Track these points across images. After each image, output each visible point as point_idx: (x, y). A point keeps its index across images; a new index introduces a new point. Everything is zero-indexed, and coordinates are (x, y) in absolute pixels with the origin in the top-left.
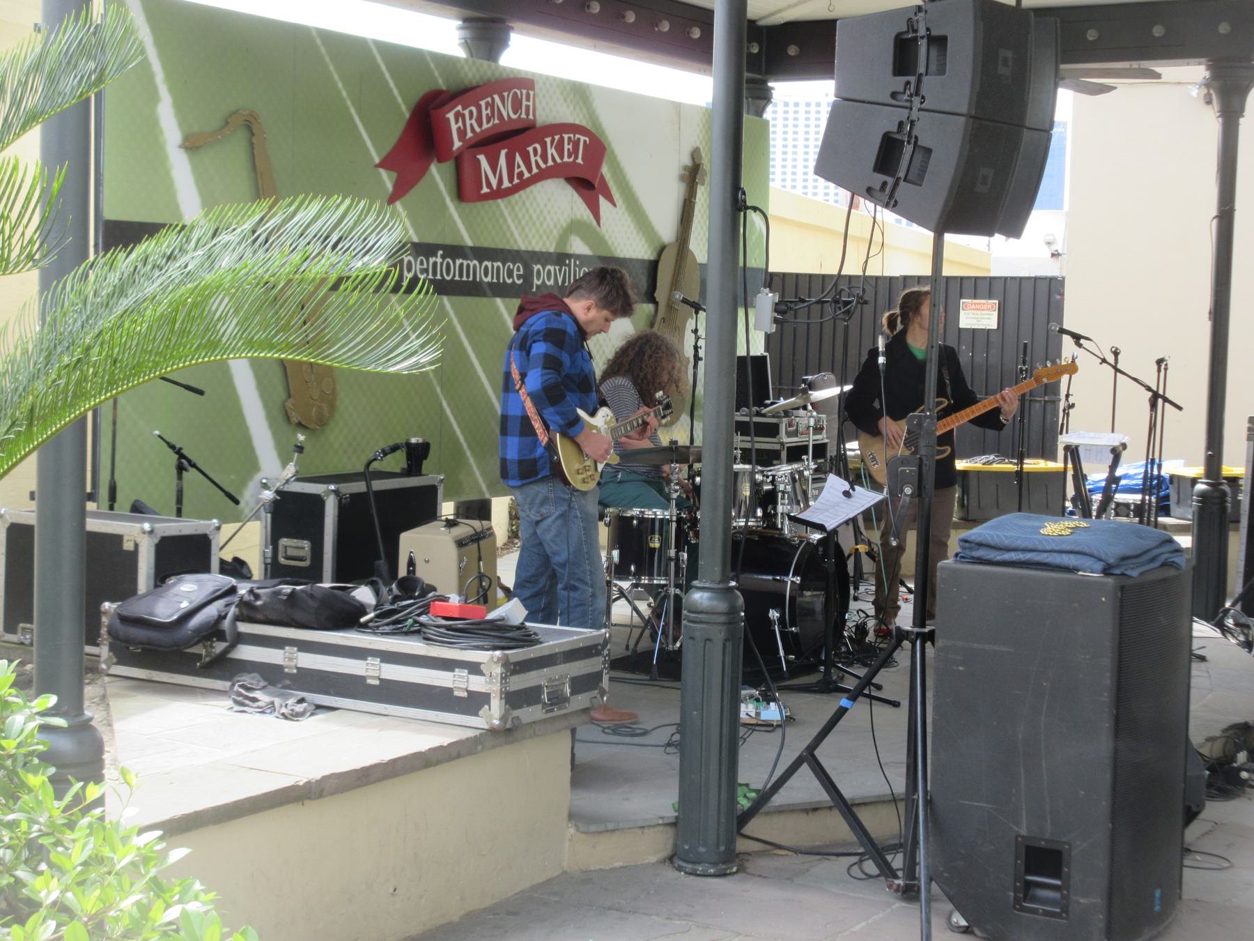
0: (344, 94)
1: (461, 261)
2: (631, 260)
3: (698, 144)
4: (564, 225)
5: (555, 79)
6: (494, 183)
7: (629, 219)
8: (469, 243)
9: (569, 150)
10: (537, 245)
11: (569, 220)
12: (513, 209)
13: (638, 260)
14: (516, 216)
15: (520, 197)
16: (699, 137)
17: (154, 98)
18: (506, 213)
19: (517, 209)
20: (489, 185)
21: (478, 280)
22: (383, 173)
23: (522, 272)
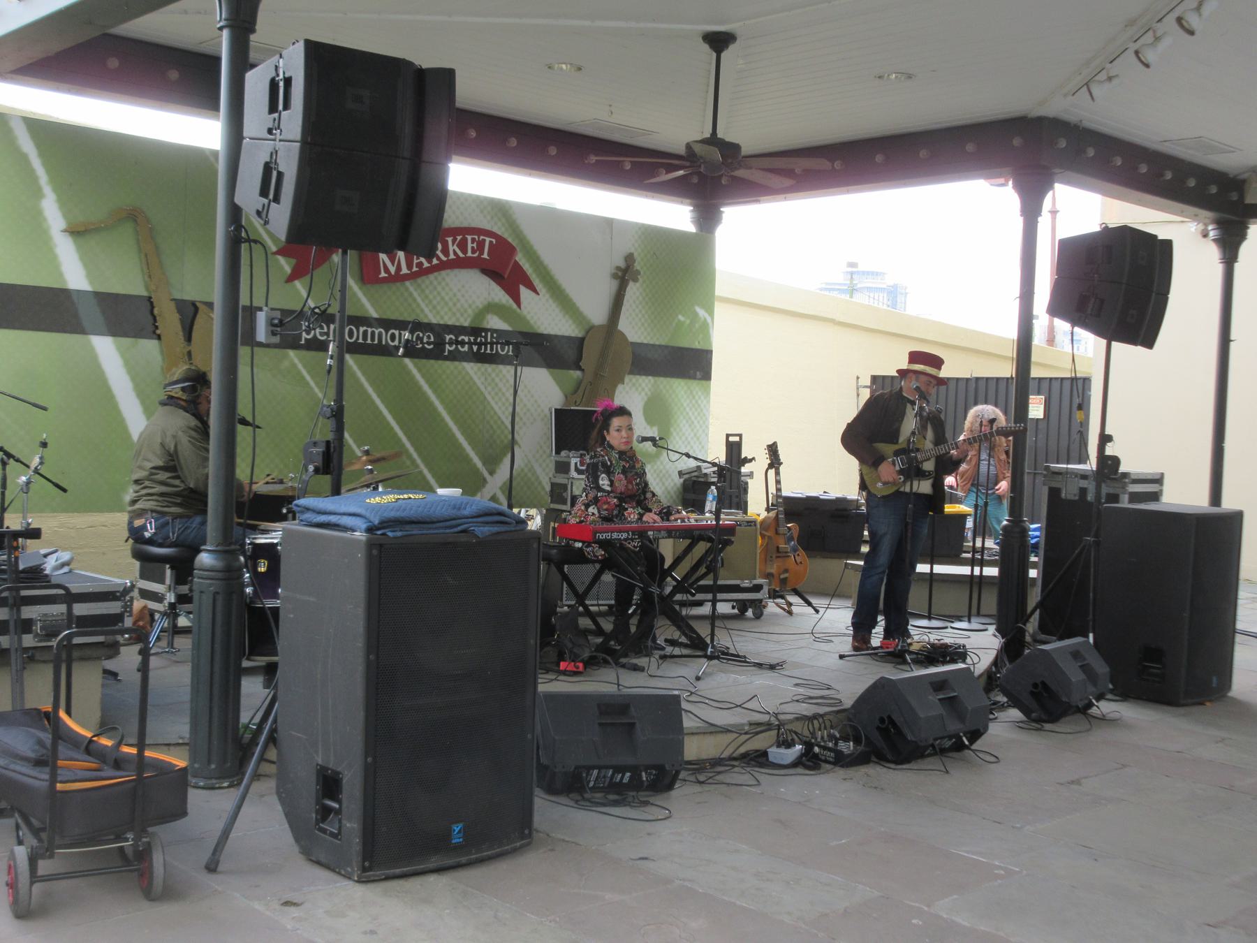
1: (365, 328)
2: (556, 336)
3: (632, 250)
4: (481, 306)
5: (470, 195)
6: (392, 270)
7: (554, 306)
8: (375, 315)
9: (473, 248)
10: (450, 320)
11: (486, 303)
12: (423, 291)
13: (563, 337)
14: (427, 297)
15: (431, 283)
16: (633, 245)
17: (38, 194)
18: (415, 294)
19: (427, 292)
20: (387, 270)
21: (384, 343)
22: (281, 260)
23: (432, 339)
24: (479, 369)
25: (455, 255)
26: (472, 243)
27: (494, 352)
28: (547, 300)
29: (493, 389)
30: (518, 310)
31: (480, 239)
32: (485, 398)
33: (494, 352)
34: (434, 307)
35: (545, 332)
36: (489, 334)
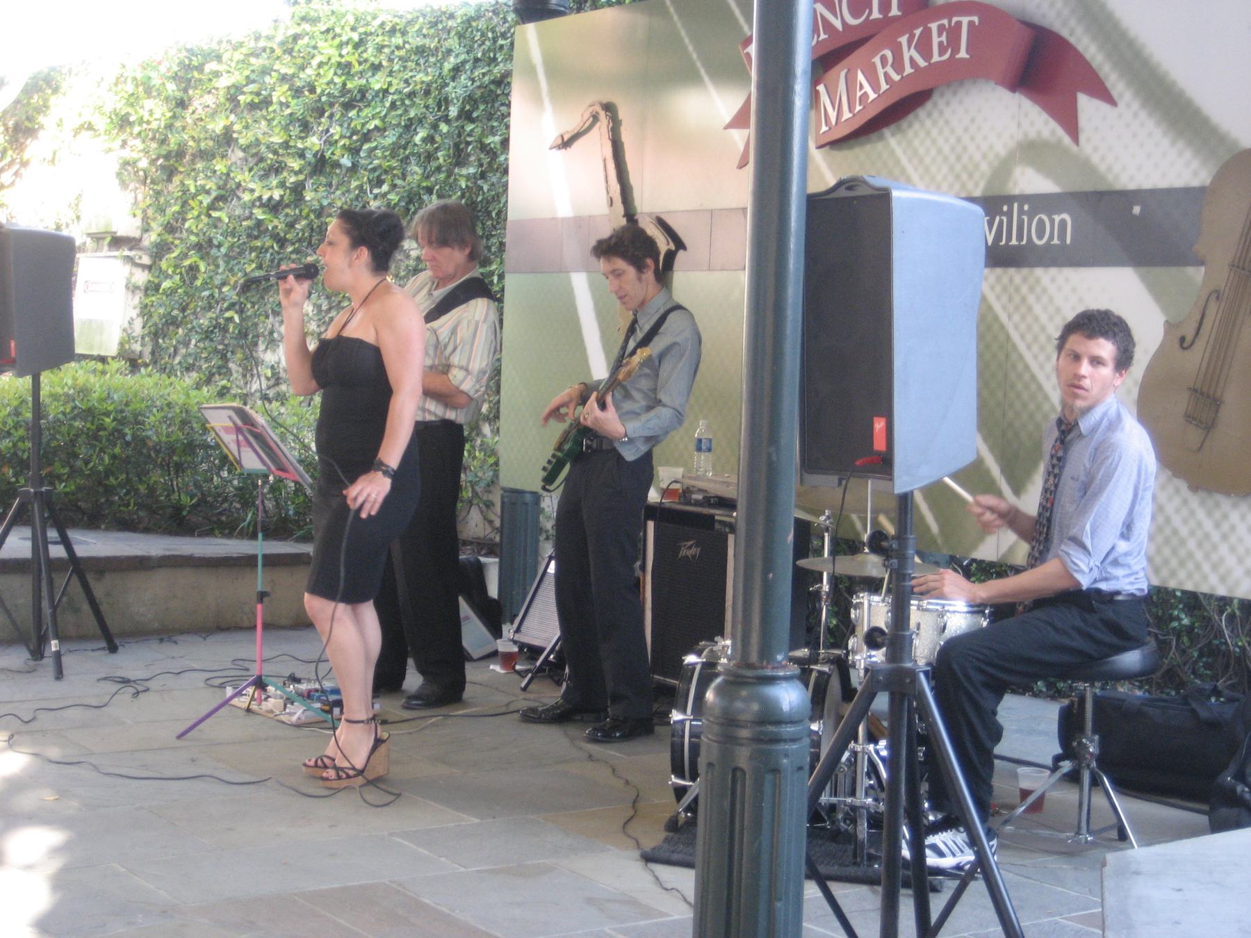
0: (695, 56)
4: (1003, 153)
7: (1150, 124)
9: (941, 44)
11: (1012, 144)
13: (1169, 192)
14: (915, 152)
19: (916, 143)
24: (999, 279)
25: (912, 67)
26: (940, 35)
27: (1024, 242)
28: (1136, 115)
29: (1023, 318)
30: (1074, 148)
31: (953, 24)
32: (1008, 337)
33: (1024, 242)
34: (927, 169)
35: (1132, 186)
36: (1016, 205)
